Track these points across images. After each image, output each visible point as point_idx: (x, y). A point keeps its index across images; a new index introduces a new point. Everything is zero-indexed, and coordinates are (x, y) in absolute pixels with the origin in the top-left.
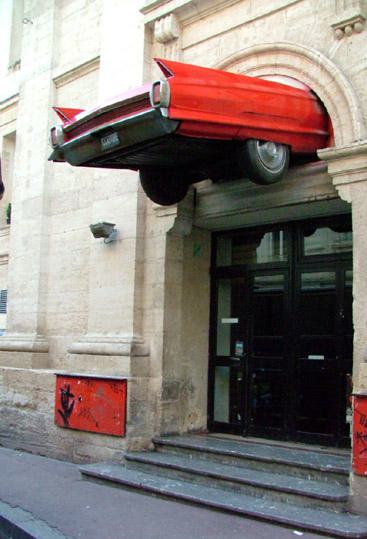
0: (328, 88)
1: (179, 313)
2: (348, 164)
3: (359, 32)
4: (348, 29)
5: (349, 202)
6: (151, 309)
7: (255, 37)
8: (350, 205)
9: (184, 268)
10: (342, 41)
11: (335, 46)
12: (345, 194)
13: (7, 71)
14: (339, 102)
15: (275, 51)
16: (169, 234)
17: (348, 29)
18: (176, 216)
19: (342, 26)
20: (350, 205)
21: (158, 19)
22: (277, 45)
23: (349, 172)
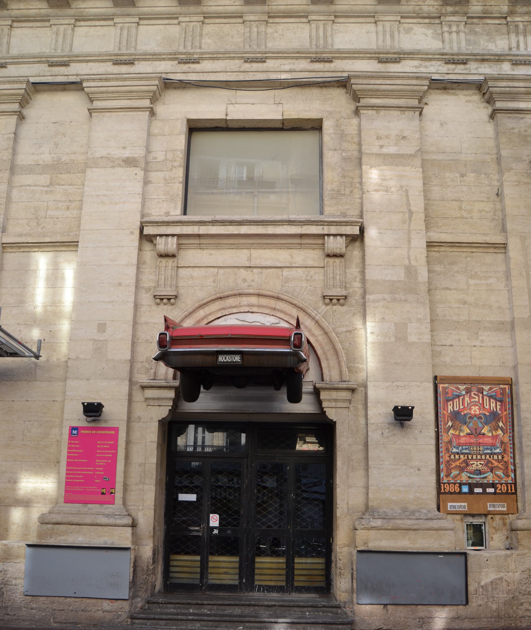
0: (320, 338)
1: (158, 487)
2: (335, 395)
3: (342, 305)
4: (335, 301)
5: (334, 420)
6: (137, 484)
7: (253, 281)
8: (335, 422)
9: (20, 380)
10: (329, 307)
11: (323, 308)
12: (331, 414)
13: (493, 541)
14: (328, 350)
15: (278, 298)
16: (162, 422)
17: (335, 301)
18: (170, 408)
19: (331, 298)
20: (335, 422)
21: (161, 236)
22: (280, 295)
23: (336, 400)
